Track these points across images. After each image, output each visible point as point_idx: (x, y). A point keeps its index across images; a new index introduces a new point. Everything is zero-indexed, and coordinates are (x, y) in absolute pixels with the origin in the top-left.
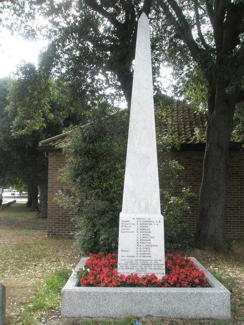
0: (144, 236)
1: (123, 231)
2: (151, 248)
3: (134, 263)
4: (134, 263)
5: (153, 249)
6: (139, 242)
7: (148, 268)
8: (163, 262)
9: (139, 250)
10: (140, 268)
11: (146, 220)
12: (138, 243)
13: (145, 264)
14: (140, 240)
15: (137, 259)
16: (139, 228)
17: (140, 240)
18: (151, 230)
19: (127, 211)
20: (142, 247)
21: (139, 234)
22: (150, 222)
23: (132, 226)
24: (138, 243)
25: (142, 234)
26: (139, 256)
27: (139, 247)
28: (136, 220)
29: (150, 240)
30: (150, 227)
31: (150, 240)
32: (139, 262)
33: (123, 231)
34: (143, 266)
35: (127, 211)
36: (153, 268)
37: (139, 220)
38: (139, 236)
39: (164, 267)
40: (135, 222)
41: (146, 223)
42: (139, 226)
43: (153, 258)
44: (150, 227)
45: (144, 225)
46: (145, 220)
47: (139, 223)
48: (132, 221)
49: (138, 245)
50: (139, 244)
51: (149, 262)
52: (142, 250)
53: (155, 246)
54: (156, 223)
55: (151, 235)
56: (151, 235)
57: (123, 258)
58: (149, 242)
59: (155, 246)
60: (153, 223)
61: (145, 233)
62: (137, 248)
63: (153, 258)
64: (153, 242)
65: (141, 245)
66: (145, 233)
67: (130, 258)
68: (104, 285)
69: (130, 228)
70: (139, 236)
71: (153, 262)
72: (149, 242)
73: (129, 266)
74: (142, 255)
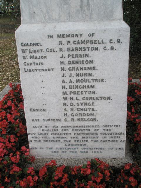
0: (80, 78)
1: (27, 68)
2: (96, 102)
3: (60, 131)
4: (60, 131)
5: (100, 107)
6: (68, 90)
7: (90, 140)
8: (123, 128)
9: (69, 108)
10: (73, 141)
11: (85, 37)
12: (64, 93)
13: (85, 133)
14: (71, 87)
15: (66, 124)
16: (66, 60)
17: (71, 87)
18: (96, 64)
19: (32, 15)
20: (75, 102)
21: (67, 73)
22: (93, 43)
23: (49, 55)
24: (64, 93)
25: (74, 73)
26: (69, 119)
27: (68, 102)
28: (56, 40)
29: (93, 87)
30: (94, 55)
31: (93, 87)
32: (70, 130)
33: (27, 68)
34: (80, 137)
35: (32, 15)
36: (99, 140)
37: (64, 40)
38: (67, 79)
39: (124, 138)
40: (54, 44)
41: (82, 46)
42: (66, 54)
43: (101, 121)
44: (94, 55)
45: (79, 52)
46: (80, 39)
47: (65, 47)
48: (47, 44)
49: (65, 99)
50: (68, 96)
51: (92, 130)
52: (75, 107)
53: (105, 98)
54: (109, 46)
55: (96, 74)
56: (96, 74)
57: (35, 124)
58: (91, 90)
59: (105, 98)
60: (101, 47)
61: (81, 72)
62: (65, 104)
63: (101, 121)
64: (100, 89)
65: (72, 99)
66: (81, 72)
67: (51, 124)
68: (21, 124)
69: (41, 61)
70: (67, 79)
71: (101, 130)
72: (91, 90)
73: (51, 137)
74: (76, 118)
